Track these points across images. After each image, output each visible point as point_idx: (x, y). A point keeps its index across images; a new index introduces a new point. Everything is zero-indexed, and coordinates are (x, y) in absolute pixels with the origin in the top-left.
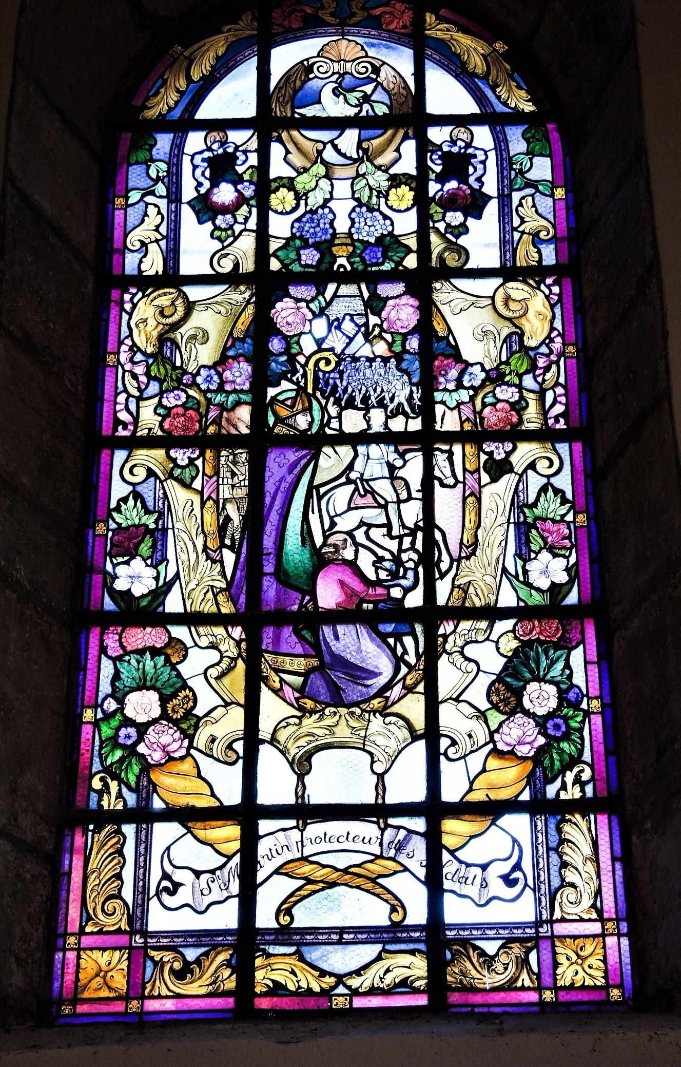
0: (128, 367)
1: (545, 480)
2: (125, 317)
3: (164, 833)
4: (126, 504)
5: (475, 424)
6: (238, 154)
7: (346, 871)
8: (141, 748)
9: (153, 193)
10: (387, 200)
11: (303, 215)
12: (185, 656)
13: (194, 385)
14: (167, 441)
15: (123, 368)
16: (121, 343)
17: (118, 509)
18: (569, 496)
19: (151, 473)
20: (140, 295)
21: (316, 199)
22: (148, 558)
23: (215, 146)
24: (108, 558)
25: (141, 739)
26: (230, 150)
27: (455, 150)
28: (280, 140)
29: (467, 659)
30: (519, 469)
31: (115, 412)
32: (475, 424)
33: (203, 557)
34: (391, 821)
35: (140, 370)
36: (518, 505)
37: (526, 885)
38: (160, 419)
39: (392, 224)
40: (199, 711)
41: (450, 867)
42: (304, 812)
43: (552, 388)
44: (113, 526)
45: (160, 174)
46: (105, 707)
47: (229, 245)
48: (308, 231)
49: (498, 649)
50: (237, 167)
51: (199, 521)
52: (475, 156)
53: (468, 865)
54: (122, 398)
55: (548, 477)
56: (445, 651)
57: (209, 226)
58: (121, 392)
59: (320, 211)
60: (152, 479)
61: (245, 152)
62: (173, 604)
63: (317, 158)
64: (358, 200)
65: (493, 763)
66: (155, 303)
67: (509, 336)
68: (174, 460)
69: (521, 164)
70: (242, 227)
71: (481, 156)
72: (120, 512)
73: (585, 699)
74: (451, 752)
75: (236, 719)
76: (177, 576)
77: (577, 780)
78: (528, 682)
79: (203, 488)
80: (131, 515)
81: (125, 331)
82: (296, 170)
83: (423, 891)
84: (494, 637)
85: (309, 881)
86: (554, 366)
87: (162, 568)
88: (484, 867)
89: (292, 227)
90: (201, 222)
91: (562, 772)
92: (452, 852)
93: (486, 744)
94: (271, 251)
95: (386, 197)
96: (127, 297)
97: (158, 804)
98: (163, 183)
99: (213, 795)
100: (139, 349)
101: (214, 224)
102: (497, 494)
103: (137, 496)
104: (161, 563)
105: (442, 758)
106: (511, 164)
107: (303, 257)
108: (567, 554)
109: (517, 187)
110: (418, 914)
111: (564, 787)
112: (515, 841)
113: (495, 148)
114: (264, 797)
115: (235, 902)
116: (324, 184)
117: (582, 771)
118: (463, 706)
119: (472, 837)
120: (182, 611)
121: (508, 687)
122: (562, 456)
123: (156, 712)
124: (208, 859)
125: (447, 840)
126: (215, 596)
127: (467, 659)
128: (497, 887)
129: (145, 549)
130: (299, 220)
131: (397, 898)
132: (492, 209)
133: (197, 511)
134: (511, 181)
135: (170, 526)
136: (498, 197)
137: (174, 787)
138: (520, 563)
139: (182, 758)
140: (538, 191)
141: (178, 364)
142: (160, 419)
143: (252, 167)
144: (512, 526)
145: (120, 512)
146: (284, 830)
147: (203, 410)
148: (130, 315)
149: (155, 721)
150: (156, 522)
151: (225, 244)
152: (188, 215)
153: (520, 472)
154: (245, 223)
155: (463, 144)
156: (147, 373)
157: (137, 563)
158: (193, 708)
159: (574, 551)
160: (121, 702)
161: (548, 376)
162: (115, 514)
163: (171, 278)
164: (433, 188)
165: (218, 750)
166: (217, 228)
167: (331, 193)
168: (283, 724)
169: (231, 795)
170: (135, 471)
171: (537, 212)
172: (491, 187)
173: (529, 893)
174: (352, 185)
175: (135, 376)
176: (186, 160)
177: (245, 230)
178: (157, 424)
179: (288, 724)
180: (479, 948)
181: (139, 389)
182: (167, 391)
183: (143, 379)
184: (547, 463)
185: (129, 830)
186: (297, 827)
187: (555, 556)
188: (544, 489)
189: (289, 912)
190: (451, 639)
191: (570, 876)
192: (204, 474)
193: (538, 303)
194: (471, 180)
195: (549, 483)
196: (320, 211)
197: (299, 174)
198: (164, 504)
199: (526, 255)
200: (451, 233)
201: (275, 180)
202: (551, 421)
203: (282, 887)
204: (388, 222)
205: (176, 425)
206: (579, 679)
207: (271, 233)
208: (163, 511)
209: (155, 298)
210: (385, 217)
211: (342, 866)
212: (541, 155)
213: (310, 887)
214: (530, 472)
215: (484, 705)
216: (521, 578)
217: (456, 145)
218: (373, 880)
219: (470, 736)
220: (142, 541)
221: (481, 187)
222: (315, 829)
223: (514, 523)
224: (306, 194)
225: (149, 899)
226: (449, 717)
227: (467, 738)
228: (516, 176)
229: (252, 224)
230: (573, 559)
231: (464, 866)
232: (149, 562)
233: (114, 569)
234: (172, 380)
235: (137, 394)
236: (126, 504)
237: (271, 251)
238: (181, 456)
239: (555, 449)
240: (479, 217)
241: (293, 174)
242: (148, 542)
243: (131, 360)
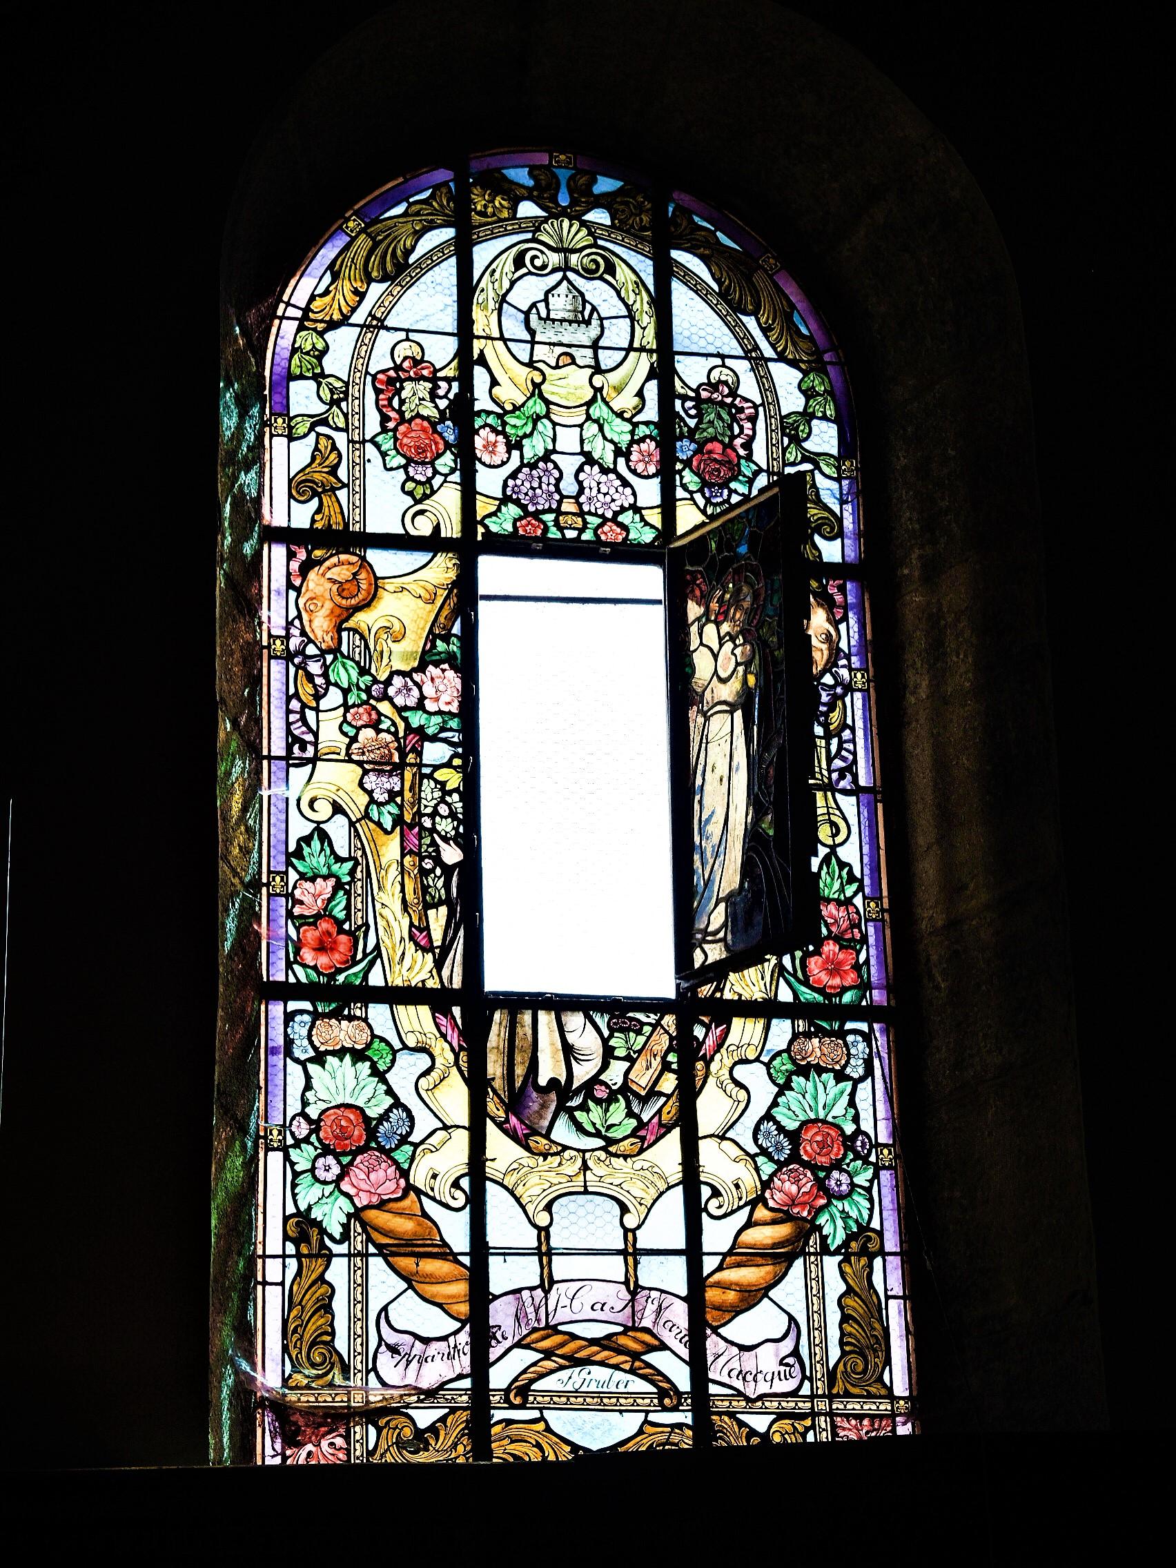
9: (324, 422)
10: (628, 461)
11: (518, 470)
12: (393, 1061)
13: (385, 697)
21: (534, 448)
38: (347, 740)
39: (634, 494)
48: (526, 494)
49: (770, 1075)
59: (541, 464)
66: (328, 575)
69: (797, 429)
74: (712, 1206)
75: (457, 1150)
89: (505, 485)
94: (479, 518)
95: (627, 455)
101: (407, 473)
105: (704, 1215)
109: (792, 459)
118: (726, 1145)
130: (514, 475)
131: (668, 1381)
142: (347, 740)
156: (325, 675)
158: (409, 1134)
166: (409, 478)
167: (554, 440)
170: (316, 805)
178: (344, 747)
183: (319, 681)
196: (541, 464)
201: (479, 413)
204: (628, 491)
207: (478, 489)
209: (329, 569)
210: (625, 483)
217: (717, 390)
219: (737, 1186)
226: (712, 1158)
229: (456, 477)
234: (359, 689)
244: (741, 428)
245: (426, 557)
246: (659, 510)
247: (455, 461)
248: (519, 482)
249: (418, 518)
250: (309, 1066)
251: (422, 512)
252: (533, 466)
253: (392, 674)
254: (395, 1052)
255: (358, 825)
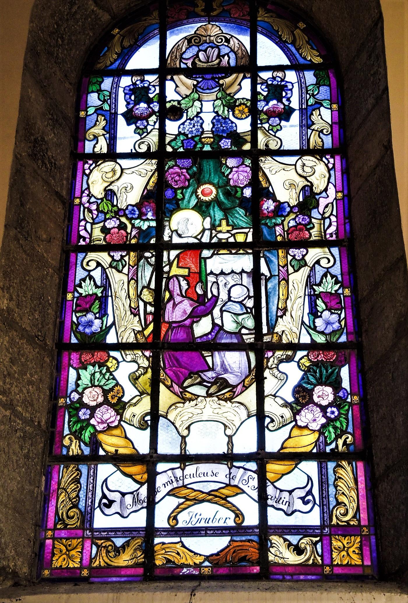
0: (87, 205)
1: (326, 270)
2: (85, 178)
3: (105, 470)
4: (85, 282)
5: (284, 238)
6: (150, 87)
7: (209, 494)
8: (93, 421)
11: (185, 121)
14: (108, 248)
15: (84, 206)
16: (82, 192)
17: (80, 286)
18: (340, 279)
19: (99, 264)
20: (94, 165)
22: (97, 313)
23: (138, 83)
24: (74, 314)
25: (92, 416)
26: (146, 85)
27: (275, 83)
28: (172, 79)
29: (280, 372)
30: (310, 263)
31: (79, 231)
32: (284, 238)
33: (129, 313)
34: (235, 464)
35: (94, 207)
36: (310, 283)
37: (315, 503)
39: (236, 126)
40: (125, 399)
41: (270, 490)
42: (184, 459)
43: (329, 217)
44: (76, 295)
45: (106, 98)
46: (72, 397)
47: (145, 137)
50: (149, 95)
51: (127, 292)
52: (287, 86)
53: (281, 491)
54: (83, 223)
55: (328, 268)
56: (267, 367)
57: (133, 127)
58: (82, 220)
60: (99, 268)
61: (154, 86)
62: (111, 338)
63: (193, 89)
64: (217, 112)
65: (296, 432)
67: (303, 188)
68: (112, 257)
69: (313, 91)
70: (152, 127)
71: (290, 87)
72: (81, 287)
73: (349, 396)
74: (271, 426)
75: (146, 404)
76: (114, 323)
77: (345, 443)
78: (315, 386)
79: (129, 272)
80: (87, 289)
81: (85, 186)
82: (182, 97)
83: (255, 507)
84: (297, 359)
85: (187, 500)
86: (330, 205)
87: (105, 319)
88: (291, 492)
89: (179, 127)
90: (129, 124)
91: (336, 439)
92: (272, 483)
93: (291, 422)
96: (87, 166)
97: (101, 453)
98: (107, 103)
99: (134, 448)
100: (92, 195)
101: (136, 126)
102: (298, 279)
103: (91, 278)
104: (104, 316)
106: (307, 91)
107: (185, 145)
108: (339, 312)
110: (252, 518)
111: (337, 446)
112: (309, 478)
113: (298, 82)
114: (163, 449)
115: (144, 511)
116: (197, 104)
117: (348, 438)
119: (283, 475)
120: (116, 342)
121: (305, 390)
122: (336, 257)
123: (101, 399)
124: (129, 485)
125: (269, 475)
126: (135, 335)
127: (280, 372)
128: (298, 505)
129: (96, 308)
130: (183, 124)
131: (238, 510)
132: (295, 117)
133: (126, 286)
134: (307, 101)
135: (110, 295)
136: (299, 110)
137: (110, 443)
138: (312, 318)
139: (116, 427)
140: (322, 105)
141: (115, 203)
143: (157, 94)
144: (307, 297)
145: (81, 287)
146: (173, 469)
147: (129, 230)
148: (88, 176)
149: (99, 405)
150: (102, 293)
151: (142, 137)
152: (121, 121)
153: (311, 266)
154: (154, 126)
155: (280, 80)
156: (97, 209)
157: (90, 316)
159: (343, 310)
160: (81, 394)
161: (327, 209)
162: (78, 289)
163: (112, 155)
164: (261, 105)
165: (136, 421)
168: (173, 407)
169: (144, 449)
170: (90, 264)
171: (321, 118)
172: (295, 104)
173: (317, 509)
174: (214, 104)
175: (90, 211)
176: (121, 90)
177: (154, 129)
178: (102, 238)
179: (177, 407)
180: (288, 540)
181: (92, 218)
182: (109, 219)
184: (327, 261)
185: (84, 469)
186: (180, 467)
187: (332, 313)
188: (325, 275)
189: (175, 518)
190: (271, 360)
191: (342, 499)
192: (129, 265)
193: (321, 168)
194: (284, 100)
195: (328, 272)
196: (195, 119)
197: (184, 98)
198: (106, 282)
199: (314, 140)
200: (272, 130)
201: (170, 102)
202: (328, 236)
203: (172, 502)
204: (234, 125)
205: (115, 238)
206: (346, 384)
208: (106, 285)
211: (207, 491)
212: (324, 85)
213: (188, 503)
214: (316, 265)
215: (290, 399)
216: (312, 327)
218: (225, 499)
219: (282, 417)
220: (93, 304)
221: (289, 104)
222: (190, 469)
223: (308, 295)
224: (187, 110)
225: (94, 509)
227: (280, 418)
228: (310, 97)
229: (157, 126)
230: (343, 316)
231: (278, 491)
232: (97, 315)
233: (77, 320)
235: (91, 221)
236: (85, 282)
237: (167, 142)
238: (117, 255)
239: (330, 252)
240: (287, 119)
241: (180, 98)
242: (97, 304)
243: (88, 201)
244: (287, 94)
245: (143, 160)
246: (250, 133)
247: (157, 119)
248: (185, 126)
249: (141, 146)
250: (80, 371)
251: (143, 143)
252: (191, 119)
253: (128, 206)
254: (118, 362)
255: (107, 270)
